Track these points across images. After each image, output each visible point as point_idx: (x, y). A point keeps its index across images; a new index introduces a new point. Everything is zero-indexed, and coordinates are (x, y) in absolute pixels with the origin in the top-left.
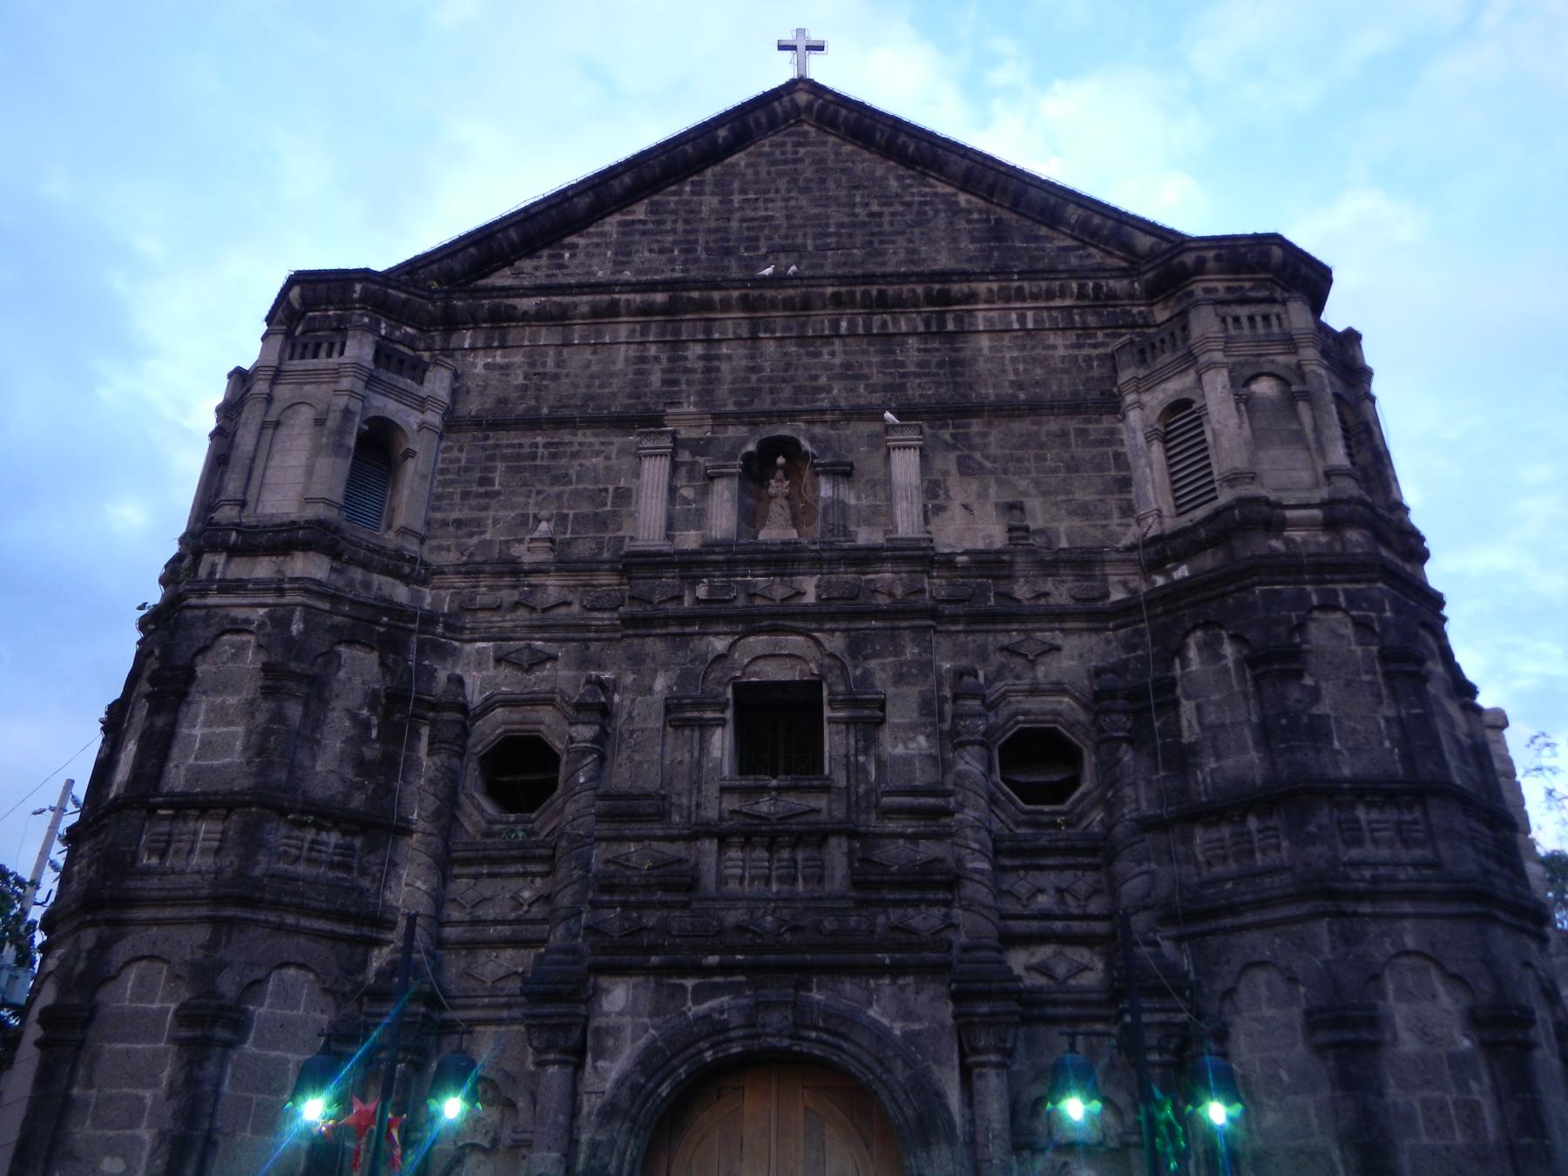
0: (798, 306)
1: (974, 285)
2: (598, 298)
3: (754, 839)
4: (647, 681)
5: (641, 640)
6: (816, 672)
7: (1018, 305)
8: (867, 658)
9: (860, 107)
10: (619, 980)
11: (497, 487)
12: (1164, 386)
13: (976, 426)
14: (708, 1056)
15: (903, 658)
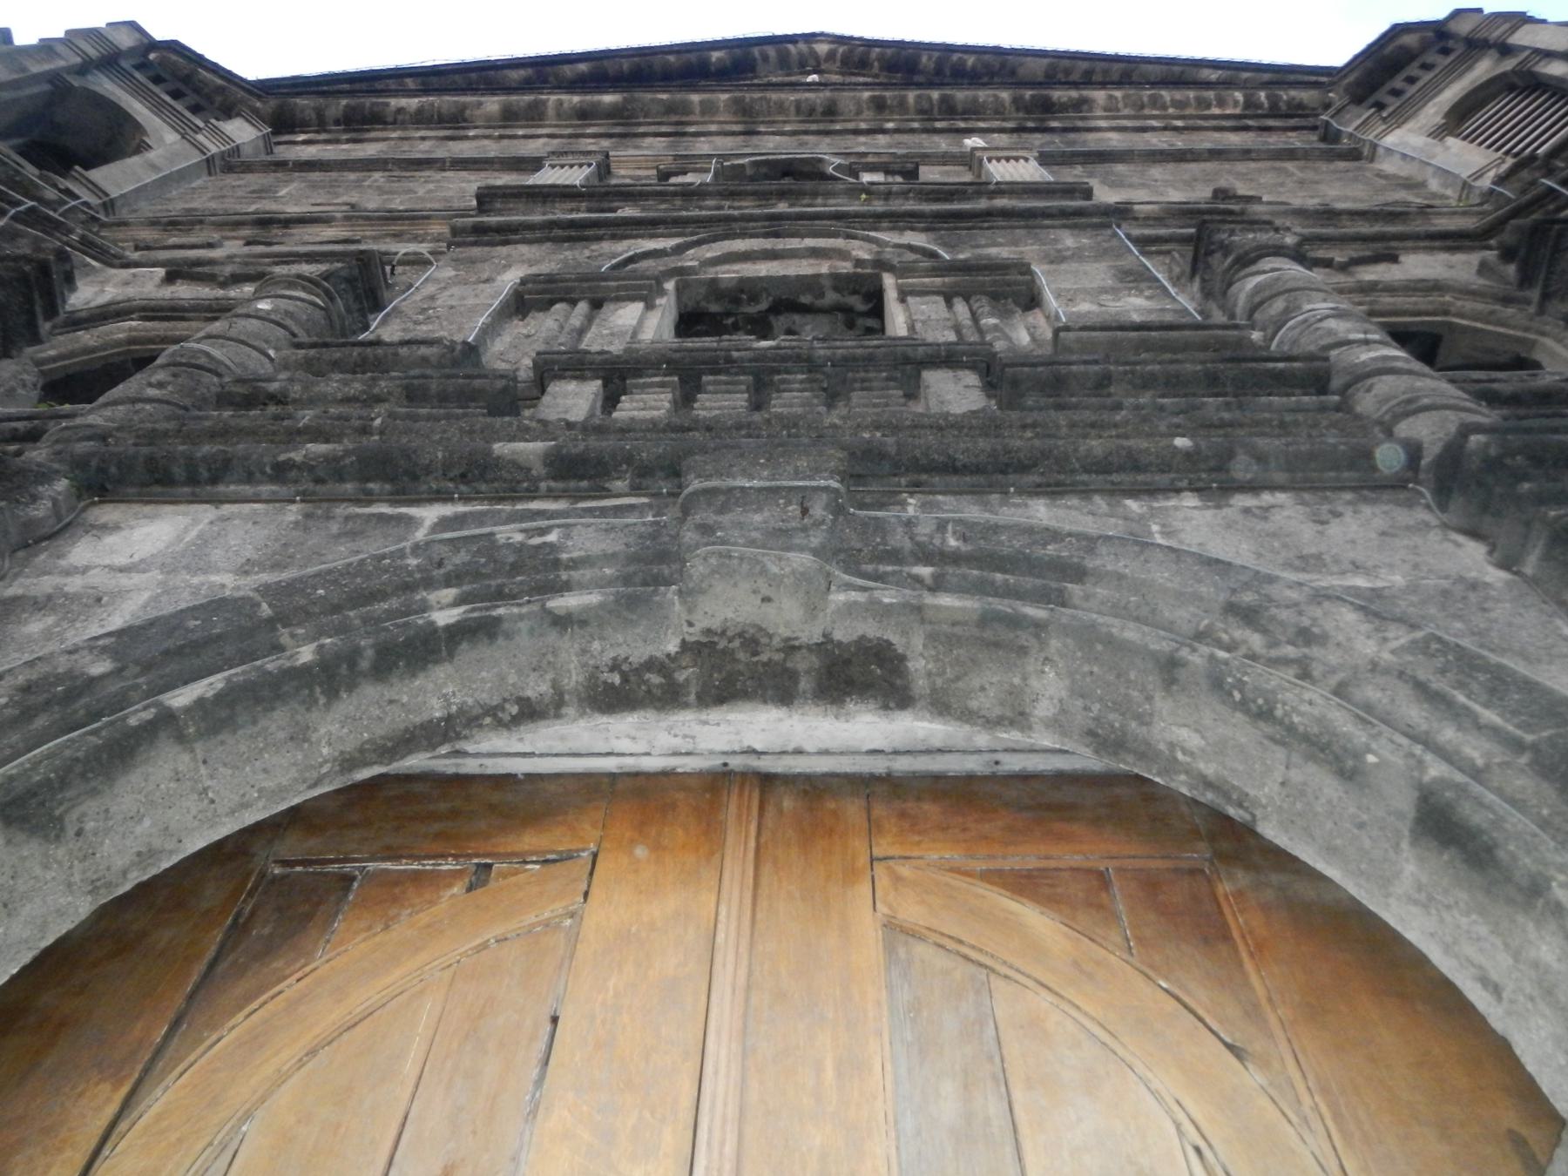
0: (820, 109)
1: (1085, 93)
2: (514, 98)
3: (705, 378)
4: (485, 276)
5: (487, 249)
6: (866, 257)
7: (1155, 112)
8: (978, 246)
9: (901, 45)
10: (168, 509)
11: (281, 194)
12: (1430, 104)
13: (1120, 168)
14: (444, 618)
15: (1059, 247)
